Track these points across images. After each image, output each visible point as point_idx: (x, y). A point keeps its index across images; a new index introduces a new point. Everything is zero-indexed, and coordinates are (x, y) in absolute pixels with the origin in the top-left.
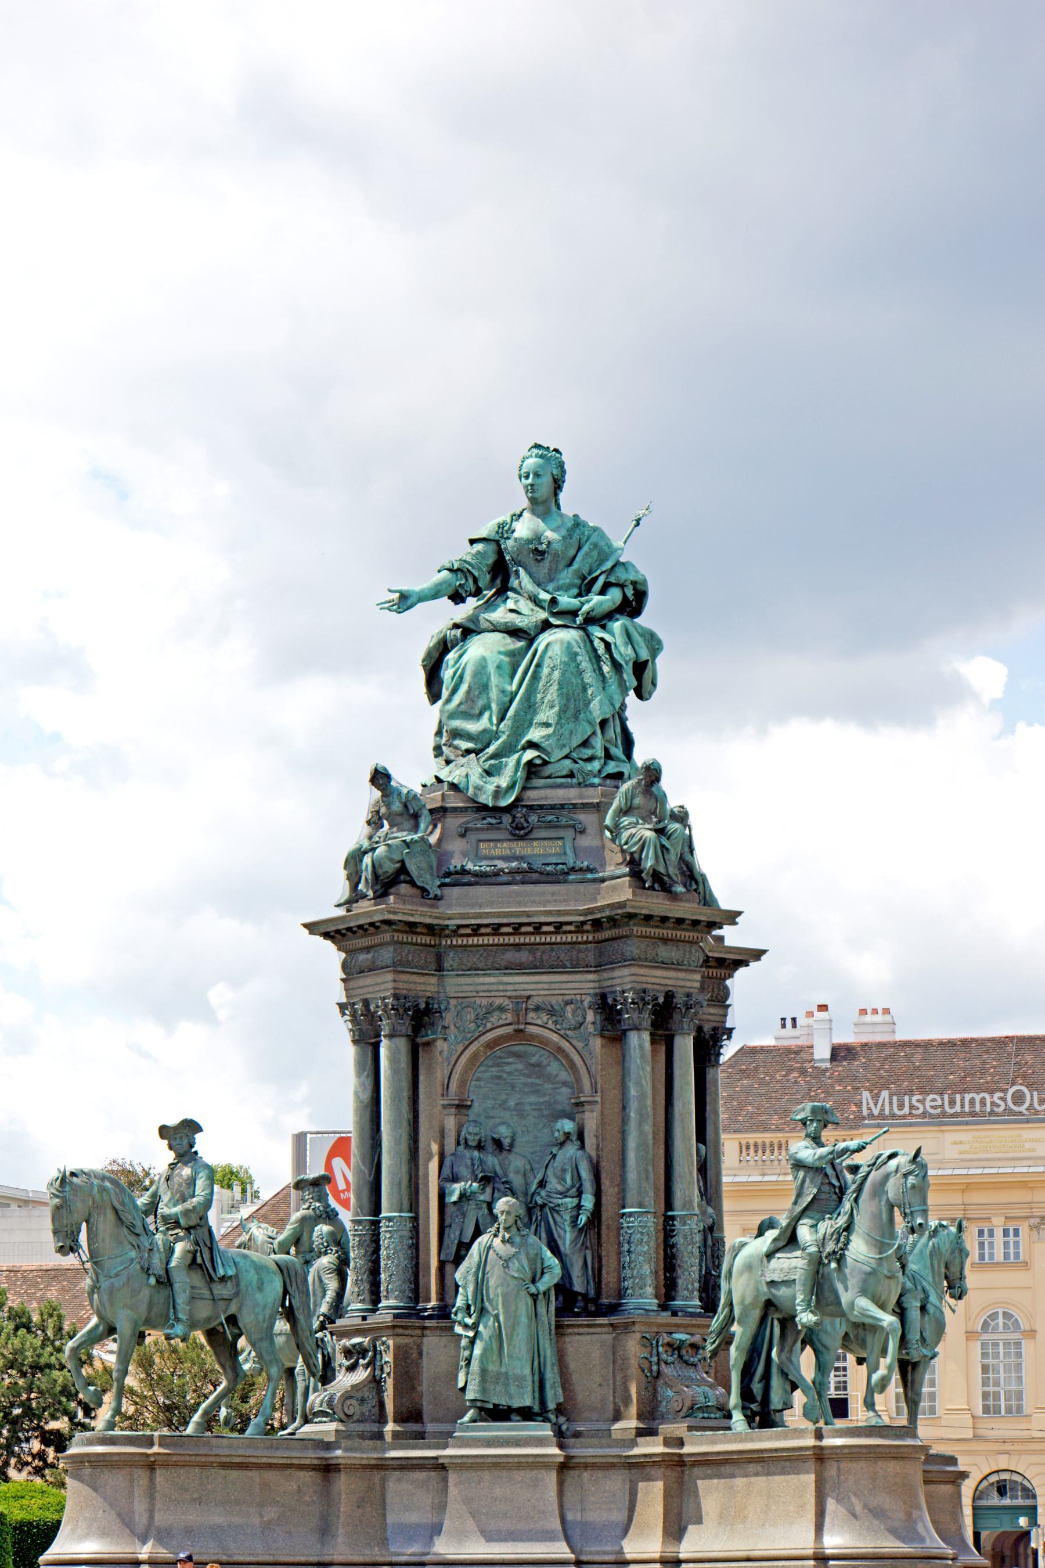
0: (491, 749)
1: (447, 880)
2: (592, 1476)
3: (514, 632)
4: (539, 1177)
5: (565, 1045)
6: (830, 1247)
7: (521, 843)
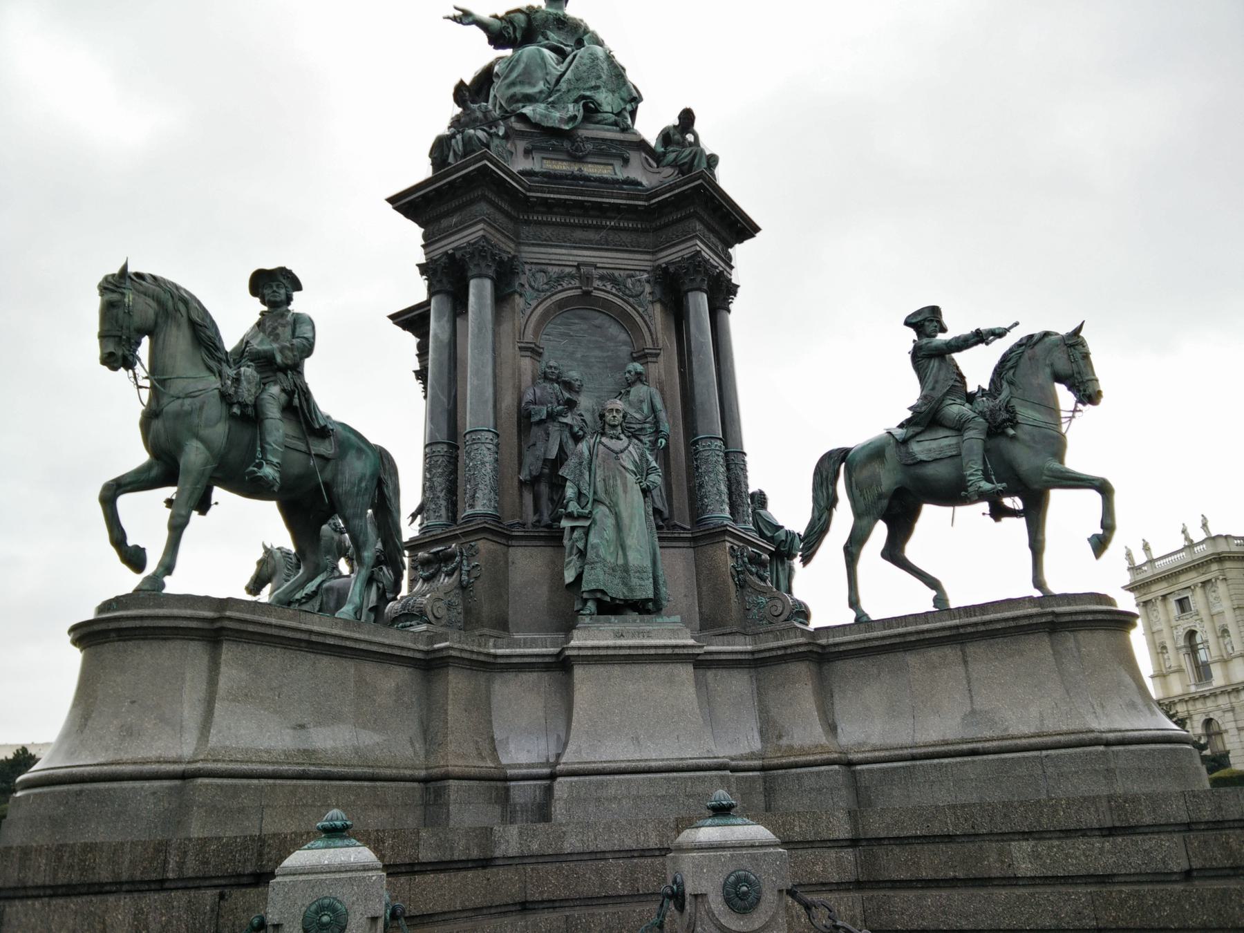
2: (716, 676)
5: (629, 309)
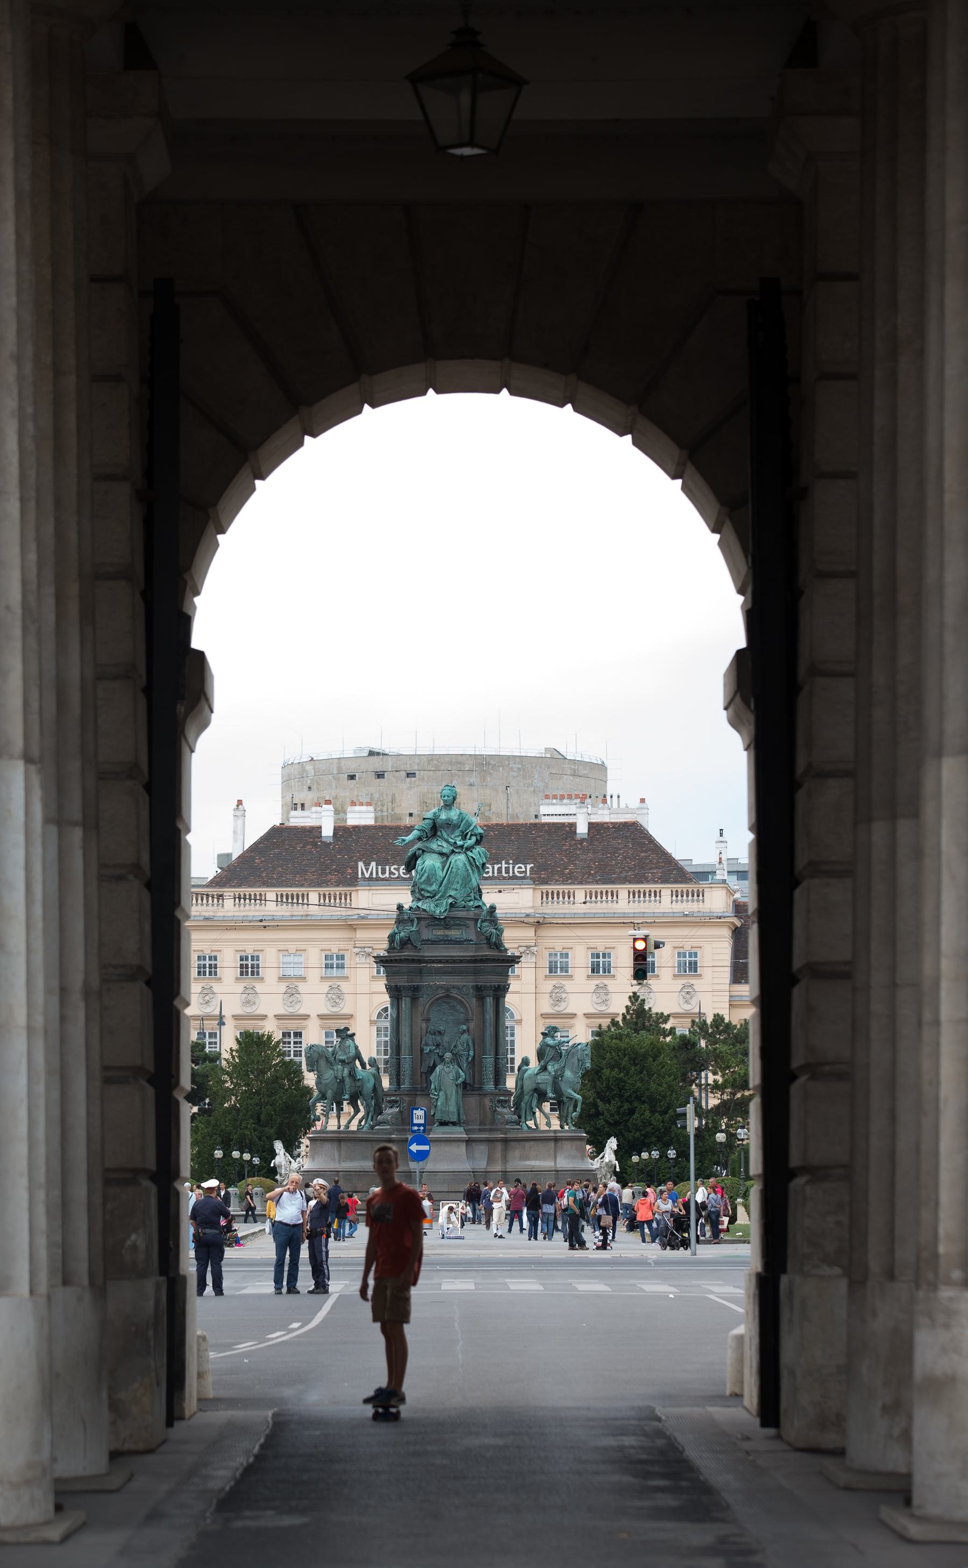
0: (437, 897)
1: (423, 943)
3: (441, 854)
4: (454, 1044)
6: (559, 1073)
7: (447, 931)
